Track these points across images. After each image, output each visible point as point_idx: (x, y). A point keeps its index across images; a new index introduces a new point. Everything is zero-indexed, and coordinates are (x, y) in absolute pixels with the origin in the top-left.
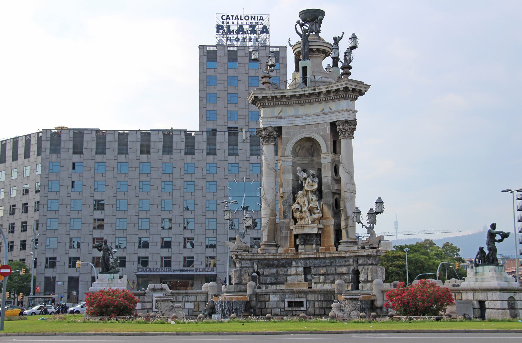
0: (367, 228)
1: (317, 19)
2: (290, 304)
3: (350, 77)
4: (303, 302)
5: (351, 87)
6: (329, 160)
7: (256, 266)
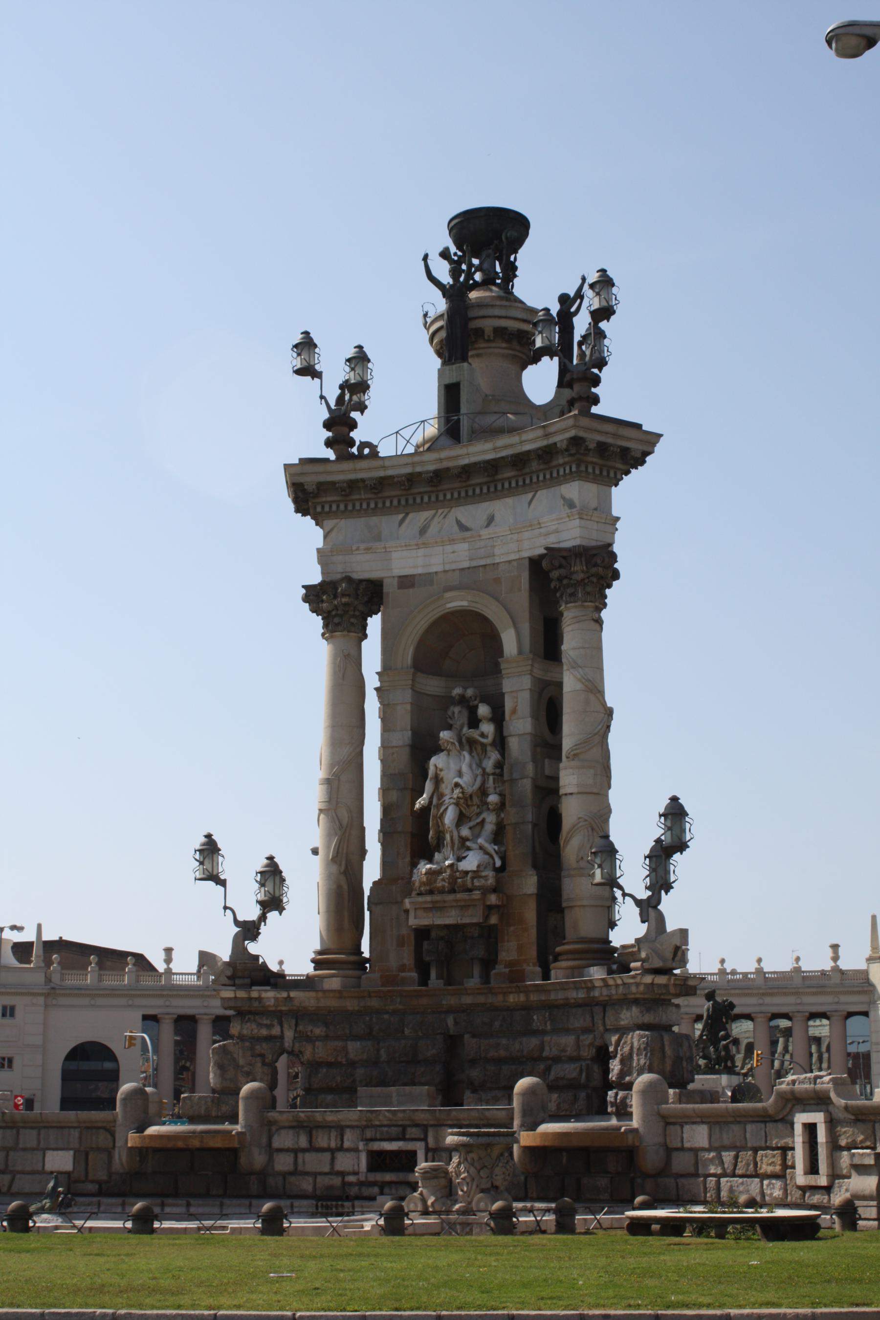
0: (638, 903)
1: (500, 239)
2: (379, 1161)
3: (595, 410)
4: (414, 1153)
5: (593, 438)
6: (526, 682)
7: (289, 1034)
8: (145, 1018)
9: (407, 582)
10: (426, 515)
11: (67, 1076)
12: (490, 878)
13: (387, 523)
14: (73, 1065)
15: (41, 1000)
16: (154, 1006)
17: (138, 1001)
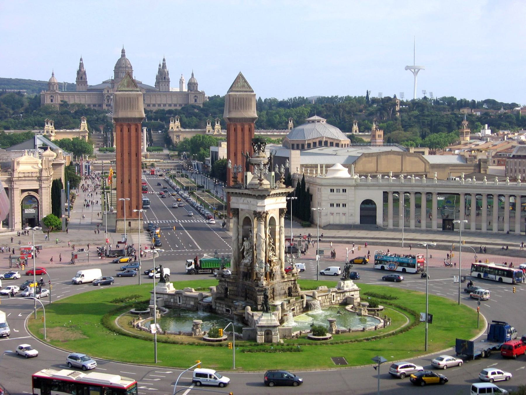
8: (384, 192)
9: (242, 210)
10: (244, 198)
11: (361, 209)
12: (249, 264)
13: (239, 198)
14: (363, 206)
15: (353, 188)
16: (386, 189)
17: (381, 188)
